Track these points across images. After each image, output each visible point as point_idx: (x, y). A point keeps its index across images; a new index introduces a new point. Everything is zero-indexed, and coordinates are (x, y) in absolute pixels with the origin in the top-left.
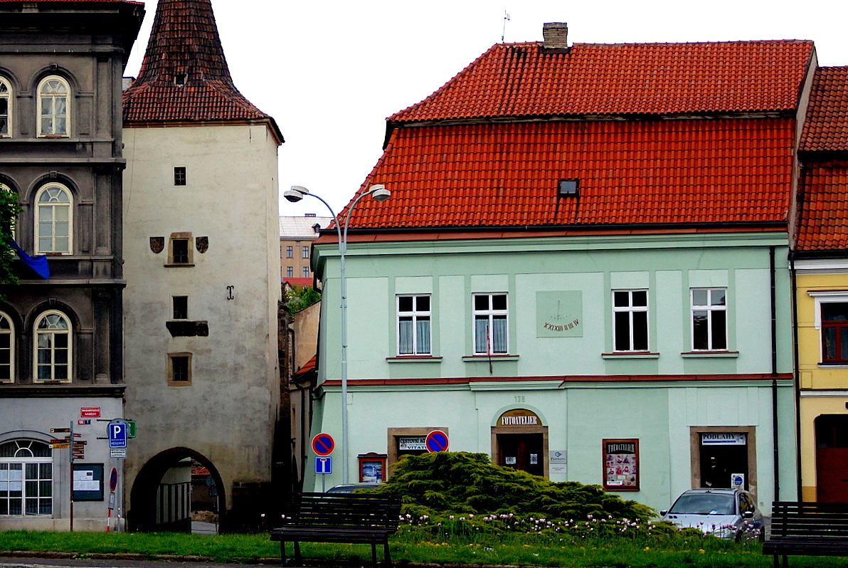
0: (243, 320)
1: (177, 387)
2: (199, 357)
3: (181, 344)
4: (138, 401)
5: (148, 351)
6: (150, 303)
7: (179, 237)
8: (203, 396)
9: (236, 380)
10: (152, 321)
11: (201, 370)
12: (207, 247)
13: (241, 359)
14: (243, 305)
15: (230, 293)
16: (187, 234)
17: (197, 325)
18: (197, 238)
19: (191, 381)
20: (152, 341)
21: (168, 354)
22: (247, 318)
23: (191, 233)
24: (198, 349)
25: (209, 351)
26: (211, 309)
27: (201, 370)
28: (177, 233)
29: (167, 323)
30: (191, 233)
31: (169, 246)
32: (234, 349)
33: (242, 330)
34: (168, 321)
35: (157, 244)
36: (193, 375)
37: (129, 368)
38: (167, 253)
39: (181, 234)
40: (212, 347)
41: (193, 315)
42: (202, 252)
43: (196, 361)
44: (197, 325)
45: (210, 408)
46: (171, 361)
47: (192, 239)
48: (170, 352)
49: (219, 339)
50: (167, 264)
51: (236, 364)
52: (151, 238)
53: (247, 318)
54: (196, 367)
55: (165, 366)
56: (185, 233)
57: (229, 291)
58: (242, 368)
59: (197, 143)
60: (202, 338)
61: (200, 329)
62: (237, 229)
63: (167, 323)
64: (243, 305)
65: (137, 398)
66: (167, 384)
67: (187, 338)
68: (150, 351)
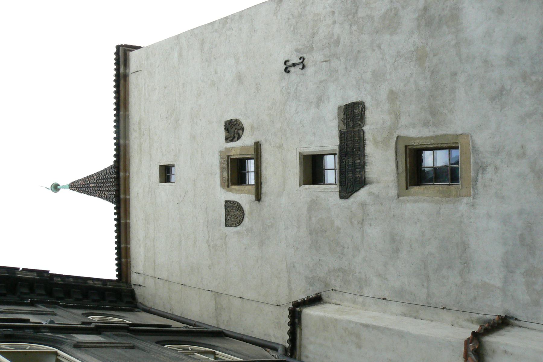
0: (337, 30)
1: (473, 174)
2: (404, 120)
3: (381, 163)
4: (506, 281)
5: (394, 242)
6: (311, 234)
7: (225, 174)
8: (493, 99)
9: (454, 17)
10: (338, 230)
11: (433, 112)
12: (236, 120)
13: (408, 19)
14: (313, 35)
15: (294, 65)
16: (221, 158)
17: (344, 129)
18: (226, 139)
19: (457, 136)
20: (375, 232)
21: (399, 196)
22: (334, 22)
23: (220, 152)
24: (389, 123)
25: (393, 96)
26: (320, 100)
27: (433, 112)
28: (221, 176)
29: (341, 197)
30: (220, 152)
31: (237, 191)
32: (387, 37)
33: (354, 28)
34: (338, 197)
35: (234, 214)
36: (441, 131)
37: (429, 296)
38: (243, 197)
39: (222, 171)
40: (383, 91)
41: (327, 140)
42: (243, 129)
43: (413, 125)
44: (344, 129)
45: (524, 77)
46: (415, 189)
47: (228, 149)
48: (393, 192)
49: (369, 76)
50: (253, 197)
51: (419, 26)
52: (226, 225)
53: (334, 22)
54: (426, 124)
55: (423, 203)
56: (221, 163)
57: (292, 69)
58: (425, 9)
59: (141, 150)
60: (368, 114)
61: (353, 116)
62: (216, 72)
63: (341, 197)
64: (313, 35)
65: (498, 283)
66: (465, 200)
67: (369, 149)
68: (393, 240)
